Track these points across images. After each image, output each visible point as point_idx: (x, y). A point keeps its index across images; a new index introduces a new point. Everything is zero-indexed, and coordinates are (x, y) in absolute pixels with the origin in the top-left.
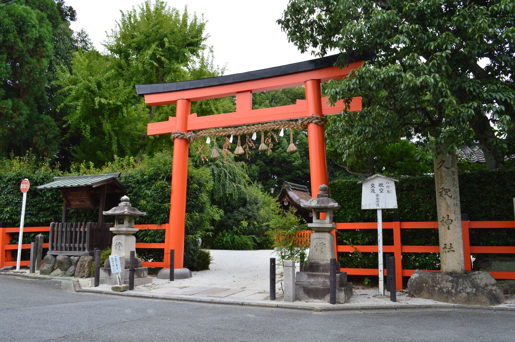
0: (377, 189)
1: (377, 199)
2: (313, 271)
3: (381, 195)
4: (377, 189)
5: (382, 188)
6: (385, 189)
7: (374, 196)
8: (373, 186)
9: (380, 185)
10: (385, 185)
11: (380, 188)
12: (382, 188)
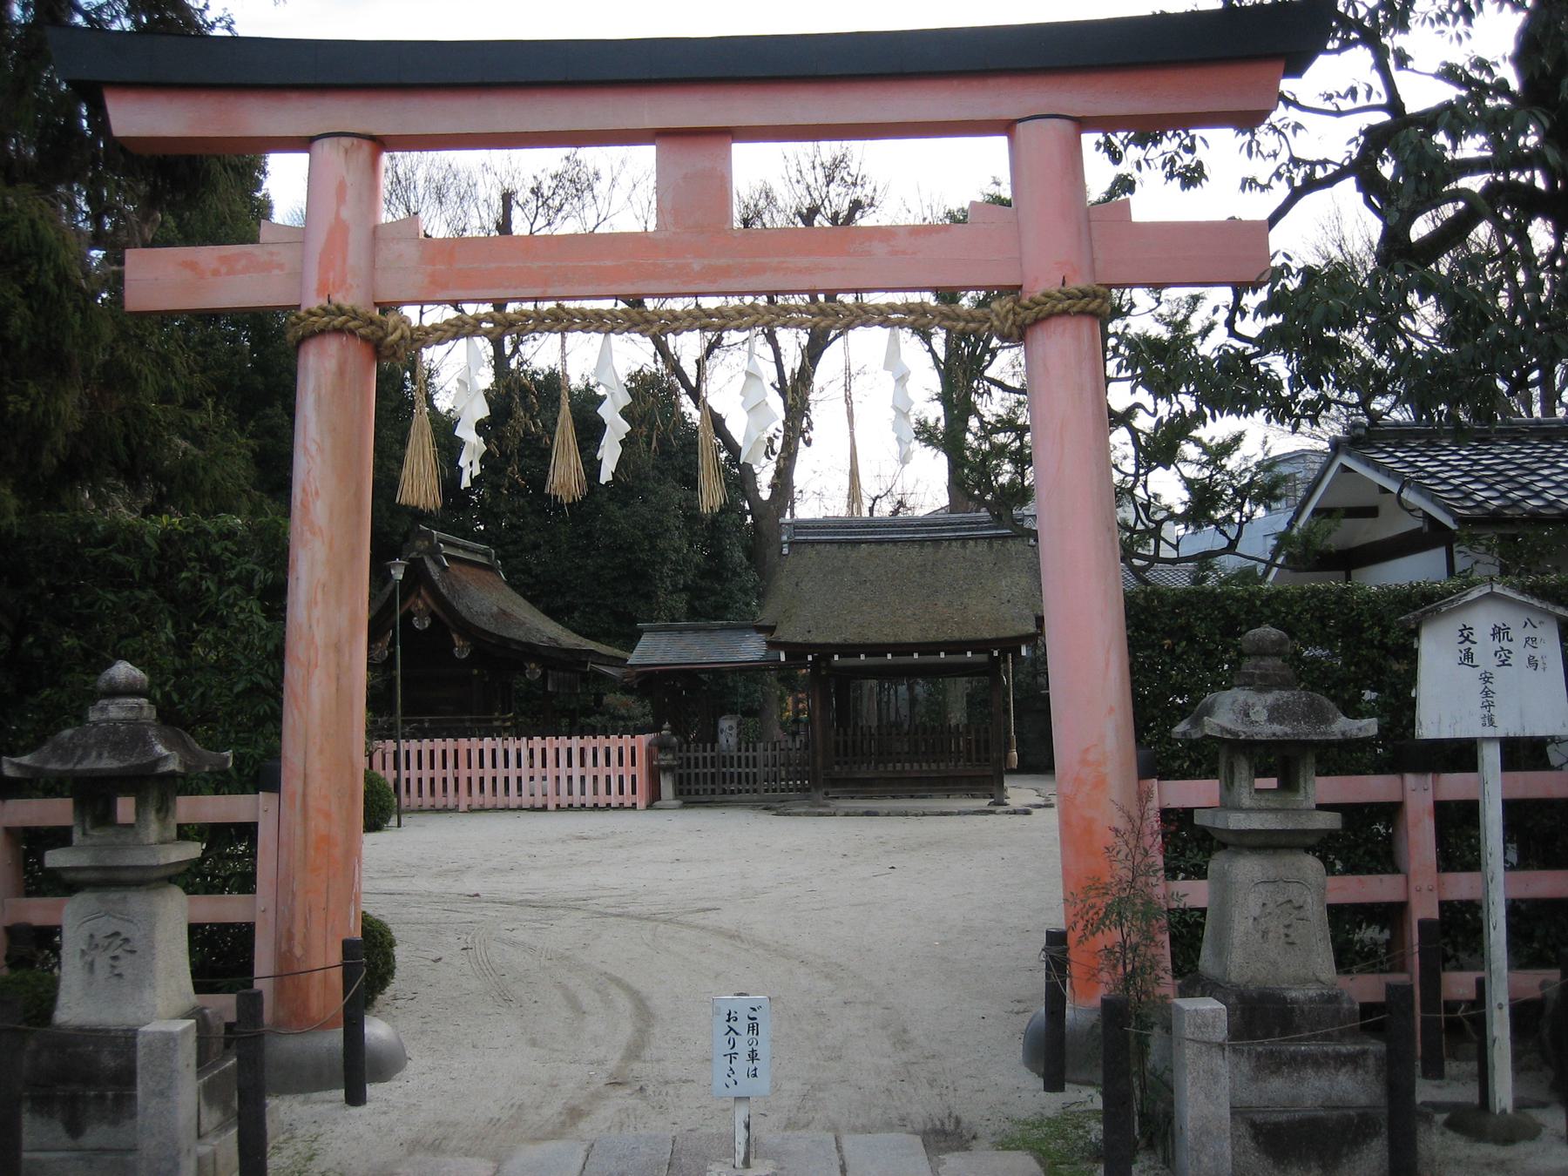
0: (1484, 647)
1: (1487, 693)
2: (1423, 1059)
3: (1501, 675)
4: (1484, 647)
5: (1505, 644)
6: (1520, 654)
7: (1470, 675)
8: (1466, 635)
9: (1499, 632)
10: (1519, 635)
11: (1496, 645)
12: (1505, 644)
